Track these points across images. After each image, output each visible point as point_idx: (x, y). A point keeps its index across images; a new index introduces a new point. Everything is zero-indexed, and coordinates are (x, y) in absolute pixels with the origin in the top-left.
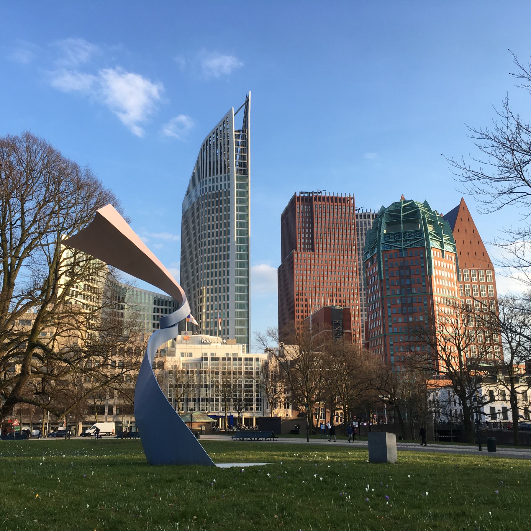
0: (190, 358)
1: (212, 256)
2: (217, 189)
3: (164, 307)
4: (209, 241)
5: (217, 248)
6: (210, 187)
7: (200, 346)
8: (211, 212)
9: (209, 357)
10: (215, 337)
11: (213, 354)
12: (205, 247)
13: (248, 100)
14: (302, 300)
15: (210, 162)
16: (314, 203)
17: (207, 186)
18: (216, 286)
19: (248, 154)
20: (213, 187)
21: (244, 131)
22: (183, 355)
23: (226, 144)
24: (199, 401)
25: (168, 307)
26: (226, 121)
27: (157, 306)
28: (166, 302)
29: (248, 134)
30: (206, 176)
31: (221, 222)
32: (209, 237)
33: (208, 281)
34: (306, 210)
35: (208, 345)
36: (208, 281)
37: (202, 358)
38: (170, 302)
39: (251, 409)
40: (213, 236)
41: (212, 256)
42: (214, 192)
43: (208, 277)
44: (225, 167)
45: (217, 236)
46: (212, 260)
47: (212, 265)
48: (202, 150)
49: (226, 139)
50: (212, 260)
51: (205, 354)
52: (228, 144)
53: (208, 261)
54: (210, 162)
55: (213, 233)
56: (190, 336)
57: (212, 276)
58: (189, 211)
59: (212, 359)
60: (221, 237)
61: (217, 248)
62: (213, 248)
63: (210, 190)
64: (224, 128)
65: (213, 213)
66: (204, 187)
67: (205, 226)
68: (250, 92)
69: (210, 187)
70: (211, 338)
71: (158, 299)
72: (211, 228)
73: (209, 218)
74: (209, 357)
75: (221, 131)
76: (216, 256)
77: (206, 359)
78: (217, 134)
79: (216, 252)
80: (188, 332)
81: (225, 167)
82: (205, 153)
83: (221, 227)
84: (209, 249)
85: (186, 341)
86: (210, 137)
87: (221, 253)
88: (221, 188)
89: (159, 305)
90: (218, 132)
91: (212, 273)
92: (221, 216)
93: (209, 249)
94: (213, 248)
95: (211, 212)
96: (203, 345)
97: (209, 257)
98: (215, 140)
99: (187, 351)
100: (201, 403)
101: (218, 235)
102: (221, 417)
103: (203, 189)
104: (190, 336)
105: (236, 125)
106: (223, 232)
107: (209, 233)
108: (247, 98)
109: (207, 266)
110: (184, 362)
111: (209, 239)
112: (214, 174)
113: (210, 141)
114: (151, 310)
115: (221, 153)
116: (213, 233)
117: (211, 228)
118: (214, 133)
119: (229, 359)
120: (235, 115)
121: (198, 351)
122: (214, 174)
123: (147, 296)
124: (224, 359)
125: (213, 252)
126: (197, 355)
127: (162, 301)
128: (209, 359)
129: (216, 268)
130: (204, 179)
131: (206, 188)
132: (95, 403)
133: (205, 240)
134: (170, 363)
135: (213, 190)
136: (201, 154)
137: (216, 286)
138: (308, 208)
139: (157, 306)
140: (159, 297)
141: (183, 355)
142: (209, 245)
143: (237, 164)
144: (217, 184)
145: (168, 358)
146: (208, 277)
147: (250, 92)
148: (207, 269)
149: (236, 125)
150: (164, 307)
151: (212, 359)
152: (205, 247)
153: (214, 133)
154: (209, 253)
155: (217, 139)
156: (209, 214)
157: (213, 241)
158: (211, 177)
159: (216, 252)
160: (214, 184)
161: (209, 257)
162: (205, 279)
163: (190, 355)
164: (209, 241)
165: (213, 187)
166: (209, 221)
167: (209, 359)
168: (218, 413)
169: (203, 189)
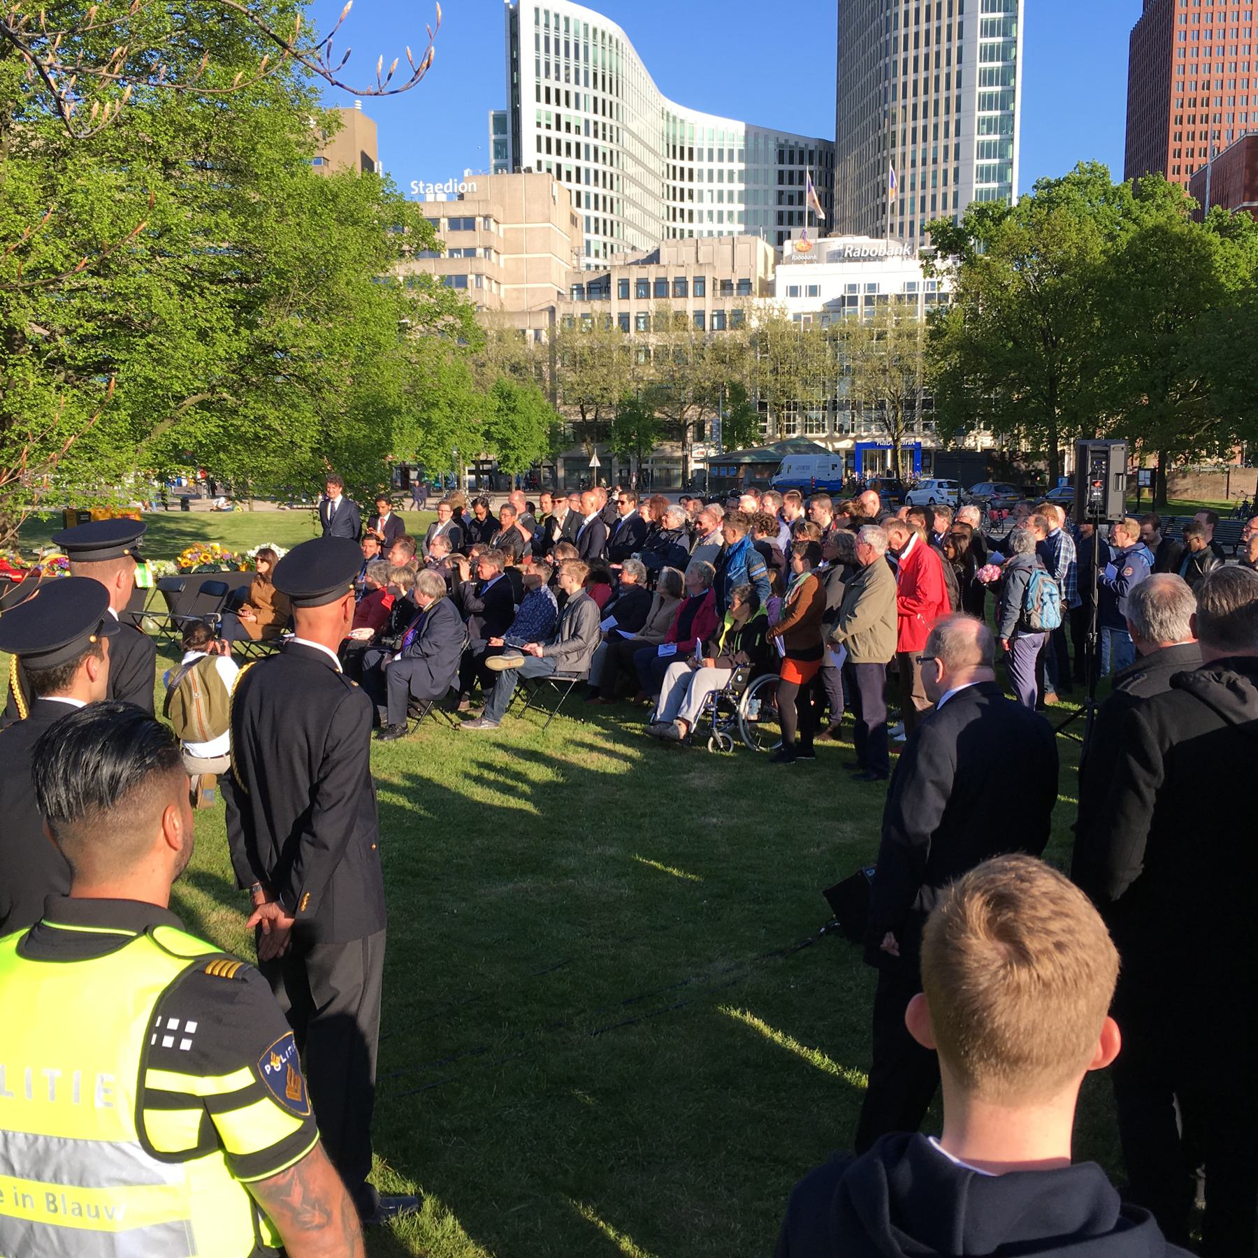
7: (838, 266)
9: (861, 295)
10: (884, 241)
11: (872, 287)
22: (794, 291)
27: (786, 167)
35: (877, 263)
37: (843, 297)
38: (811, 153)
51: (852, 287)
56: (812, 241)
70: (874, 245)
71: (780, 145)
74: (861, 295)
85: (809, 257)
89: (791, 162)
96: (847, 264)
102: (889, 447)
104: (812, 241)
114: (774, 177)
119: (913, 298)
121: (833, 281)
123: (761, 141)
124: (899, 298)
126: (832, 291)
127: (801, 153)
128: (861, 301)
132: (584, 417)
134: (758, 312)
139: (786, 167)
141: (794, 291)
145: (757, 301)
151: (869, 300)
163: (813, 291)
167: (861, 301)
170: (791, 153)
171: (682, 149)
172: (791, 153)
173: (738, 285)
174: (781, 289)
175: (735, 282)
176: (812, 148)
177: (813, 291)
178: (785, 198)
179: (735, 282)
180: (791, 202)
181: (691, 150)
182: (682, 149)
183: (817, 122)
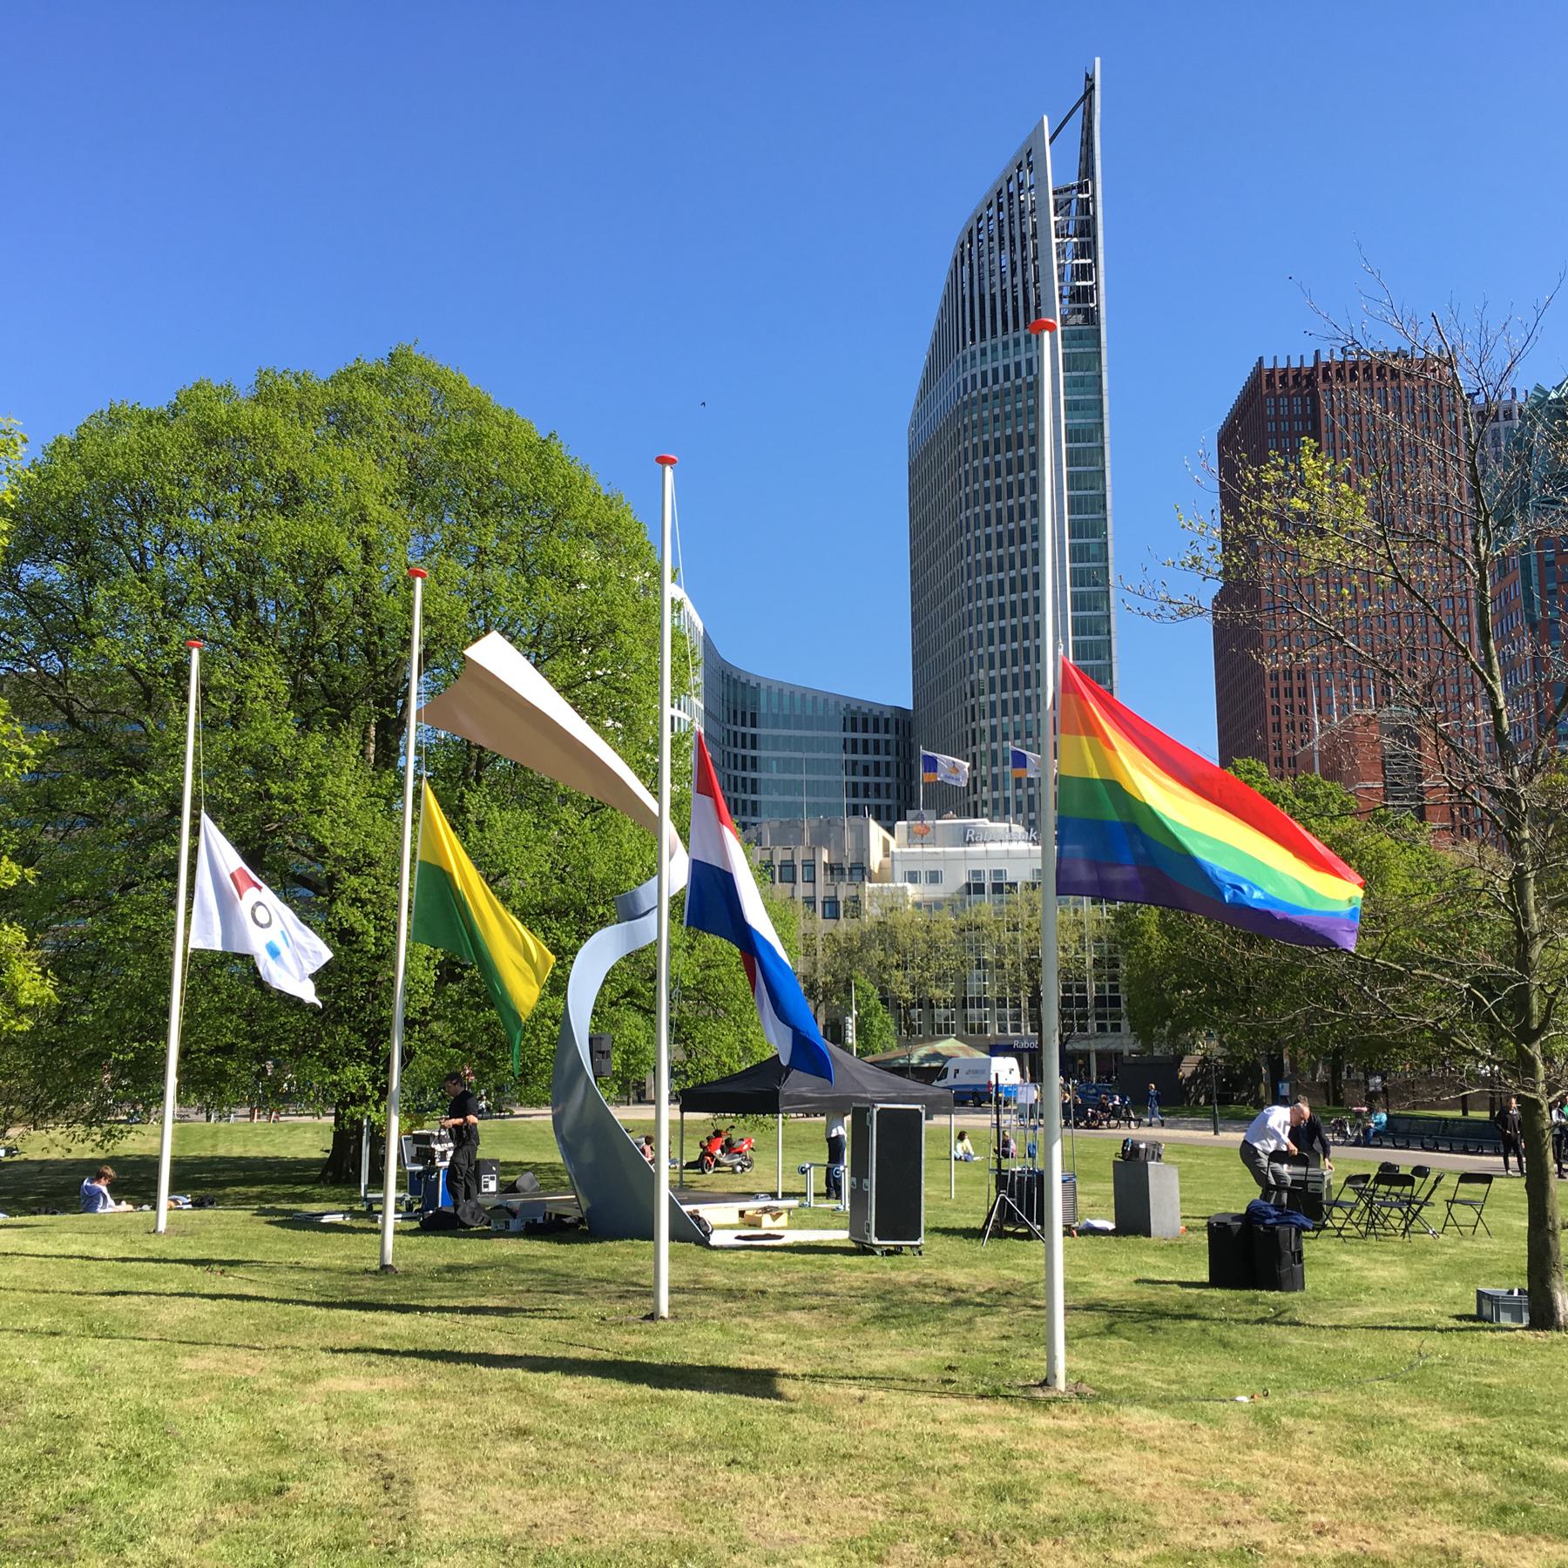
0: (933, 887)
1: (1001, 582)
2: (1007, 378)
3: (870, 736)
4: (988, 537)
5: (1012, 556)
6: (984, 374)
8: (992, 449)
11: (998, 873)
12: (978, 556)
13: (1093, 87)
14: (1289, 692)
15: (982, 297)
16: (1322, 386)
17: (977, 371)
18: (1016, 670)
19: (1095, 261)
20: (995, 371)
21: (1082, 188)
22: (913, 877)
23: (1028, 237)
24: (965, 1006)
25: (881, 736)
26: (1028, 160)
27: (850, 735)
28: (876, 721)
29: (1093, 196)
30: (973, 339)
31: (1021, 476)
32: (988, 524)
33: (991, 656)
34: (1298, 410)
36: (991, 656)
37: (968, 885)
38: (887, 720)
39: (1116, 1028)
40: (999, 522)
41: (1001, 582)
42: (996, 388)
43: (991, 643)
44: (1027, 309)
45: (1011, 519)
46: (1001, 593)
47: (1002, 606)
48: (959, 261)
49: (1029, 220)
50: (1001, 593)
51: (977, 873)
52: (1034, 236)
53: (990, 595)
54: (982, 297)
55: (999, 511)
57: (1003, 641)
58: (927, 451)
59: (998, 888)
60: (1023, 523)
61: (1012, 556)
62: (1000, 558)
63: (984, 384)
64: (1021, 186)
65: (997, 452)
66: (967, 375)
67: (976, 492)
68: (1098, 60)
69: (984, 374)
71: (853, 712)
72: (993, 498)
73: (986, 467)
75: (1010, 195)
76: (1012, 580)
77: (979, 889)
78: (1000, 208)
79: (1012, 567)
80: (925, 813)
81: (1027, 309)
82: (966, 269)
83: (1022, 493)
84: (989, 561)
86: (979, 220)
87: (1024, 571)
88: (1018, 375)
90: (1004, 200)
91: (1002, 630)
92: (1021, 459)
93: (989, 561)
94: (1000, 558)
95: (992, 449)
97: (990, 584)
98: (993, 225)
99: (923, 868)
100: (969, 1011)
101: (1016, 517)
103: (965, 380)
104: (928, 822)
105: (1054, 170)
106: (1028, 505)
107: (988, 514)
108: (1089, 79)
109: (985, 610)
110: (918, 898)
111: (988, 530)
112: (994, 332)
113: (979, 230)
115: (1013, 263)
116: (999, 511)
117: (993, 498)
118: (990, 206)
120: (1051, 141)
122: (994, 332)
125: (1000, 569)
129: (1013, 615)
130: (967, 352)
131: (974, 377)
133: (978, 533)
135: (996, 381)
136: (955, 273)
137: (1016, 670)
138: (1304, 406)
139: (850, 735)
140: (854, 708)
142: (988, 548)
143: (1066, 292)
144: (1006, 362)
146: (991, 643)
147: (1098, 60)
148: (985, 618)
149: (1054, 170)
150: (870, 736)
151: (998, 888)
152: (978, 556)
153: (990, 206)
154: (989, 572)
155: (1000, 221)
156: (986, 454)
157: (999, 535)
158: (988, 344)
159: (1012, 567)
160: (995, 364)
161: (990, 584)
162: (981, 651)
164: (988, 537)
165: (995, 371)
166: (987, 477)
168: (1021, 1039)
169: (965, 380)
170: (865, 721)
171: (744, 714)
172: (865, 721)
173: (851, 870)
174: (899, 874)
175: (847, 865)
176: (887, 715)
177: (934, 877)
178: (860, 768)
179: (847, 865)
180: (866, 773)
181: (753, 715)
182: (744, 714)
183: (893, 688)
